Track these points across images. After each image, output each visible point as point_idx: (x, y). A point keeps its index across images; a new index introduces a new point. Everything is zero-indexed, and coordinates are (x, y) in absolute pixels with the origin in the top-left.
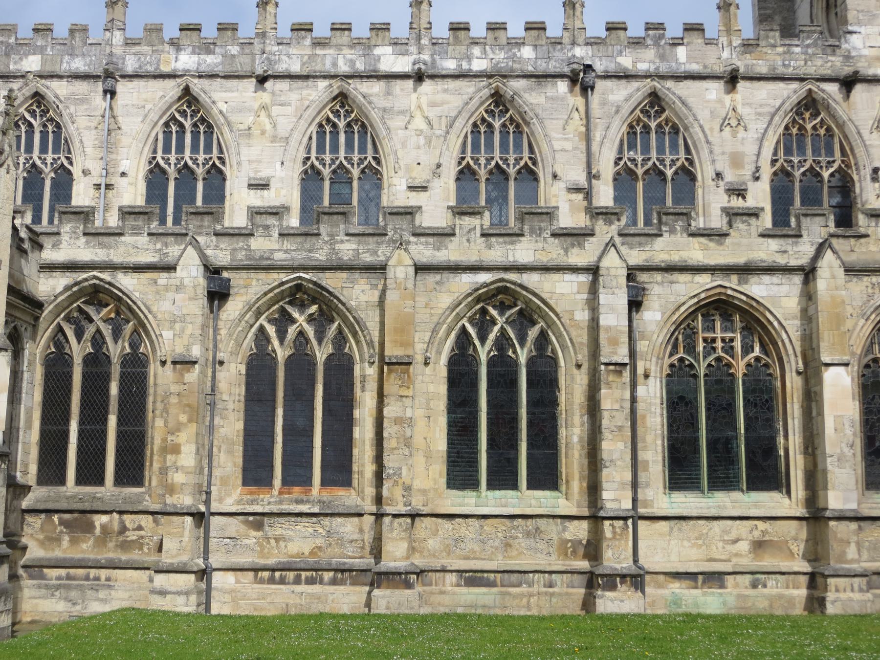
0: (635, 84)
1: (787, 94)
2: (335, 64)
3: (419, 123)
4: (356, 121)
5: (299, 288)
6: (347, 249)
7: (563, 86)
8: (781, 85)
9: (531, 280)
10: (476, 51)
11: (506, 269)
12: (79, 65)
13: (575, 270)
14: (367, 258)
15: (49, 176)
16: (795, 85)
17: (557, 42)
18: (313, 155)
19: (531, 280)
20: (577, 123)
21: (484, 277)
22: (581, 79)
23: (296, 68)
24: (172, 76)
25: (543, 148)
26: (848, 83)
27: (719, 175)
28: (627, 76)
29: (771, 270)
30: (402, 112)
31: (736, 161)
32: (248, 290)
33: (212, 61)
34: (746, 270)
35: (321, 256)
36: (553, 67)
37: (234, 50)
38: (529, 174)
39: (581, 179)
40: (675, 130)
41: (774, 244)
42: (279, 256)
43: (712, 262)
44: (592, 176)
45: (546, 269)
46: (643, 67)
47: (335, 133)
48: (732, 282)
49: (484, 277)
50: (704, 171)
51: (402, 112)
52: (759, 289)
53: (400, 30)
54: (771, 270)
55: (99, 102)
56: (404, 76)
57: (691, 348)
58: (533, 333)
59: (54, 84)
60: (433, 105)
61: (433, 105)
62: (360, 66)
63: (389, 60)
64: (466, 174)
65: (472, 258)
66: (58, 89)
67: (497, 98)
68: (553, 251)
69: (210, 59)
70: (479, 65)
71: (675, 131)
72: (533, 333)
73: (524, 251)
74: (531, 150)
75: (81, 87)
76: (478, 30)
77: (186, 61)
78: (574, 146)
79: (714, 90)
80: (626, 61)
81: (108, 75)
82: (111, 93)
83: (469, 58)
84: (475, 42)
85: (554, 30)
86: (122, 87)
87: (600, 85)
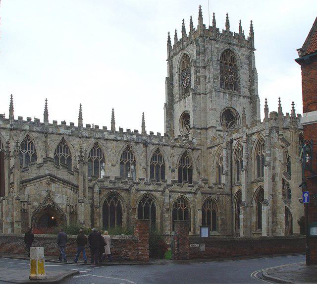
0: (155, 146)
1: (181, 151)
2: (95, 135)
3: (113, 151)
4: (99, 149)
5: (113, 192)
6: (121, 185)
7: (141, 145)
8: (181, 149)
9: (153, 193)
10: (125, 135)
11: (149, 191)
12: (39, 129)
13: (159, 191)
14: (125, 187)
15: (31, 155)
16: (185, 150)
17: (140, 135)
18: (91, 156)
19: (153, 193)
20: (144, 154)
21: (145, 192)
22: (146, 144)
23: (87, 135)
24: (60, 134)
25: (137, 159)
26: (193, 150)
27: (170, 167)
28: (154, 144)
29: (190, 193)
30: (109, 148)
31: (173, 164)
32: (106, 192)
33: (69, 131)
34: (186, 193)
35: (117, 186)
36: (140, 140)
37: (74, 129)
38: (134, 164)
39: (144, 165)
40: (161, 156)
41: (190, 188)
42: (109, 186)
43: (180, 191)
44: (147, 165)
45: (155, 191)
46: (157, 142)
47: (95, 151)
48: (184, 195)
49: (145, 192)
50: (167, 165)
51: (109, 148)
52: (188, 196)
53: (109, 129)
54: (190, 193)
55: (43, 139)
56: (110, 140)
57: (176, 206)
58: (152, 203)
59: (33, 133)
60: (116, 147)
61: (116, 147)
62: (101, 136)
63: (107, 136)
64: (122, 163)
65: (142, 189)
66: (33, 135)
67: (128, 146)
68: (156, 188)
69: (69, 131)
70: (125, 139)
71: (161, 157)
72: (152, 203)
73: (151, 188)
74: (134, 158)
75: (39, 135)
76: (125, 131)
77: (62, 131)
78: (141, 156)
79: (169, 149)
80: (153, 141)
81: (46, 133)
82: (46, 137)
83: (123, 137)
84: (124, 133)
85: (140, 132)
86: (50, 136)
87: (149, 146)
